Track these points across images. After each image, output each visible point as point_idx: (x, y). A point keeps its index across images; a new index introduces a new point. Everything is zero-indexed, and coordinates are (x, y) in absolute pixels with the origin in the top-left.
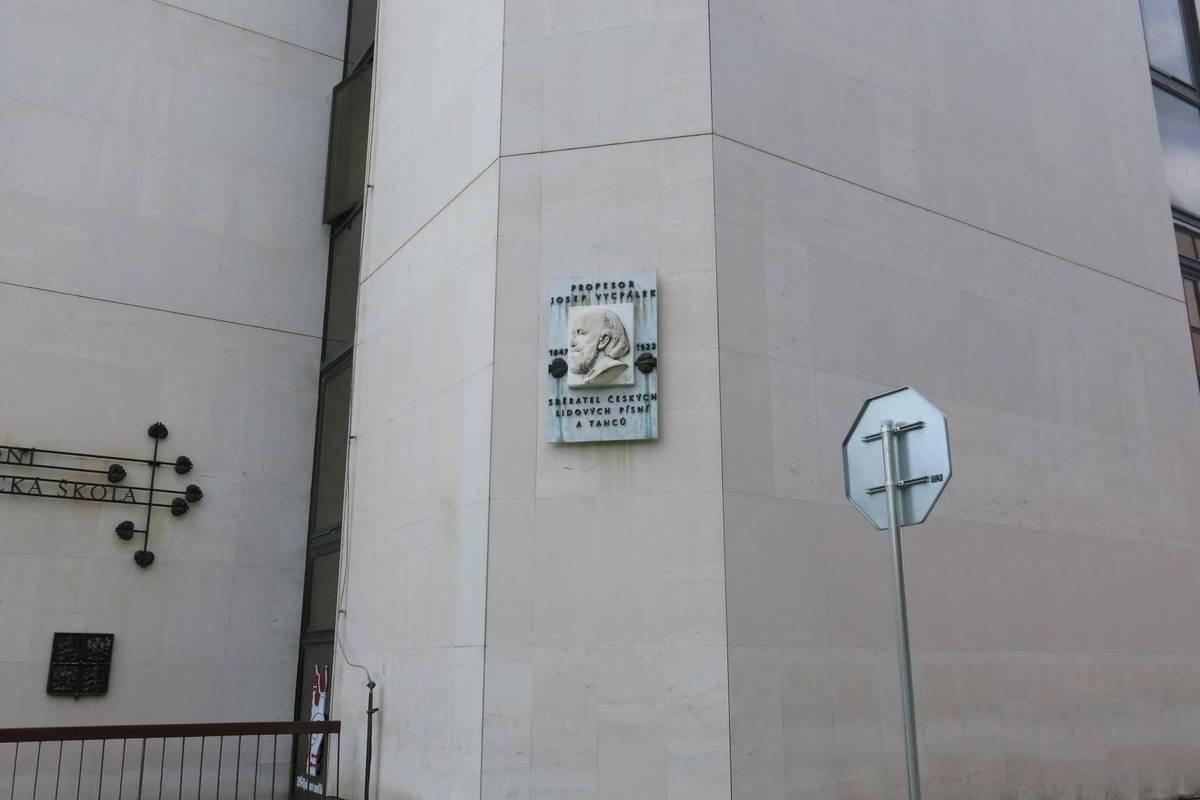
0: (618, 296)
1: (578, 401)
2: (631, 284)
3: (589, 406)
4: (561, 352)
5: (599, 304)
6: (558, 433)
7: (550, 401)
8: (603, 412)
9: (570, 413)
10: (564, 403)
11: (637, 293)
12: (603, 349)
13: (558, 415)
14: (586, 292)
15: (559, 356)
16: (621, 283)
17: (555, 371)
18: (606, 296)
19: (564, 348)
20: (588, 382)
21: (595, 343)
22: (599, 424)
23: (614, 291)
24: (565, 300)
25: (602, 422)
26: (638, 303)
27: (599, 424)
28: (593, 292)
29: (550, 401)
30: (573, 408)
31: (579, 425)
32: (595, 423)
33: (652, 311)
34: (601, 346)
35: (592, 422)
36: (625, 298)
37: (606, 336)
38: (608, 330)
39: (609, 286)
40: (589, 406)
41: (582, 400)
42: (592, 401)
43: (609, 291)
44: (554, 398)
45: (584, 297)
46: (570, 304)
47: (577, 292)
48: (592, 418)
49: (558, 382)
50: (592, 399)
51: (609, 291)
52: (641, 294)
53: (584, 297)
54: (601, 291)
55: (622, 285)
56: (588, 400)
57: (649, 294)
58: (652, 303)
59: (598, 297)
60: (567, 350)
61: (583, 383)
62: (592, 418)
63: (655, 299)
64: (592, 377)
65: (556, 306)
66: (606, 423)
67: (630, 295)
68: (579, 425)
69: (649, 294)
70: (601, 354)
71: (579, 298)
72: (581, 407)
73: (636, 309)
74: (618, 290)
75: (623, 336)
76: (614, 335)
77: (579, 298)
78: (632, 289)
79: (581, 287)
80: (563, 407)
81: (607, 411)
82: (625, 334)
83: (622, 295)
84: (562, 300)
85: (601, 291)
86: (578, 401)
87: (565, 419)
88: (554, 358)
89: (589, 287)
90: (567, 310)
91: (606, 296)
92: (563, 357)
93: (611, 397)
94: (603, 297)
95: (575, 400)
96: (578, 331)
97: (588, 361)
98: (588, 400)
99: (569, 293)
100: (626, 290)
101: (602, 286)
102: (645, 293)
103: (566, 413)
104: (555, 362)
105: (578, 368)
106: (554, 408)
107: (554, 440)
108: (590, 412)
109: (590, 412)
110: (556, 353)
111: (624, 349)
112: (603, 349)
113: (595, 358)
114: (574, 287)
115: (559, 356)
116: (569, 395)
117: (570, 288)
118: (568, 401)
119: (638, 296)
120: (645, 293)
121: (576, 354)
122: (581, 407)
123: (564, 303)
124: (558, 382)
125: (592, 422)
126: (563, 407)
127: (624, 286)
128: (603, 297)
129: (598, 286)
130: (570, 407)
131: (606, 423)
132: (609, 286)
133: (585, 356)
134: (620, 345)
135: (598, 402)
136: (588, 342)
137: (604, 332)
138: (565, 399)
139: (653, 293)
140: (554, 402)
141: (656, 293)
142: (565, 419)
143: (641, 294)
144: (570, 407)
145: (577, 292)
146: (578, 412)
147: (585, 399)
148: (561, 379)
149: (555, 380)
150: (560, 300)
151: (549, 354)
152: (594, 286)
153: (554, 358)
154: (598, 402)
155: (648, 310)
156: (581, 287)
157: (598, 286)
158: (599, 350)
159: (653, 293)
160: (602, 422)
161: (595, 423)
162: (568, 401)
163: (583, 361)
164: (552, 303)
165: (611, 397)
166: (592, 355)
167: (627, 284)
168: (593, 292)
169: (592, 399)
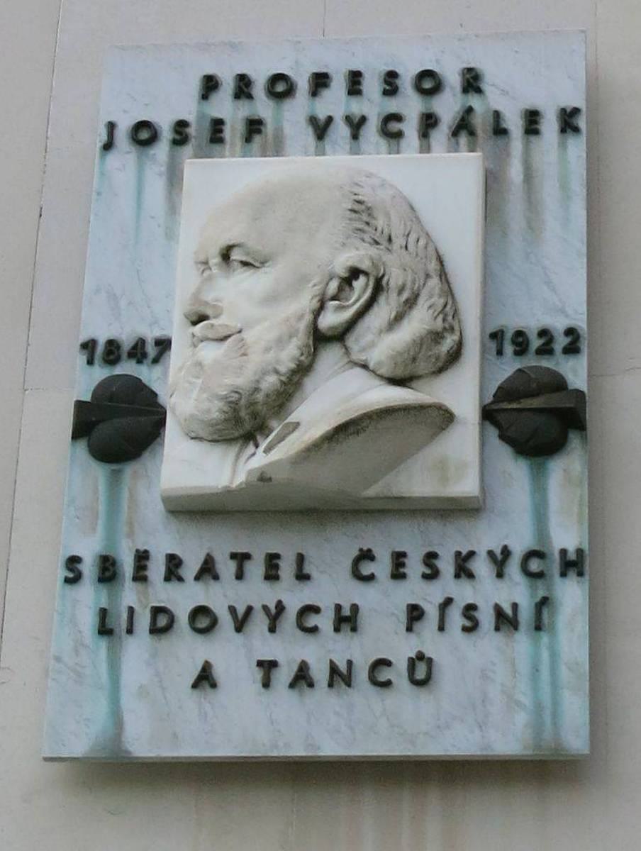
0: (410, 128)
1: (208, 570)
2: (472, 81)
3: (257, 592)
4: (138, 352)
5: (320, 152)
6: (99, 710)
7: (73, 562)
8: (325, 621)
9: (162, 623)
10: (140, 576)
11: (497, 115)
12: (340, 336)
13: (105, 630)
14: (263, 107)
15: (127, 368)
16: (426, 74)
17: (104, 430)
18: (356, 125)
19: (151, 334)
20: (263, 478)
21: (306, 302)
22: (302, 677)
23: (393, 105)
24: (167, 134)
25: (320, 673)
26: (505, 154)
27: (302, 677)
28: (299, 107)
29: (73, 562)
30: (182, 598)
31: (205, 678)
32: (284, 675)
33: (564, 186)
34: (331, 319)
35: (268, 667)
36: (440, 135)
37: (355, 273)
38: (373, 251)
39: (372, 86)
40: (257, 592)
41: (226, 568)
42: (272, 575)
43: (372, 105)
44: (89, 551)
45: (254, 127)
46: (188, 149)
47: (224, 106)
48: (269, 647)
49: (115, 482)
50: (272, 562)
51: (372, 105)
52: (515, 124)
53: (254, 127)
54: (334, 102)
55: (429, 83)
56: (256, 569)
57: (550, 125)
58: (563, 160)
59: (321, 129)
60: (164, 345)
61: (240, 478)
62: (269, 647)
63: (577, 148)
64: (278, 454)
65: (125, 151)
66: (340, 677)
67: (464, 126)
68: (205, 678)
69: (550, 125)
70: (330, 356)
71: (233, 131)
72: (219, 597)
73: (492, 183)
74: (411, 105)
75: (434, 282)
76: (395, 277)
77: (233, 131)
78: (474, 101)
79: (243, 87)
80: (129, 595)
81: (347, 620)
82: (443, 275)
83: (429, 122)
84: (154, 138)
85: (334, 102)
86: (208, 570)
87: (138, 648)
88: (100, 373)
89: (280, 87)
90: (174, 177)
91: (356, 125)
92: (146, 374)
93: (367, 555)
94: (341, 131)
95: (191, 567)
96: (226, 255)
97: (271, 382)
98: (256, 569)
99: (187, 107)
100: (448, 106)
101: (339, 85)
102: (532, 120)
103: (143, 621)
104: (103, 390)
105: (216, 410)
106: (89, 596)
107: (79, 746)
108: (259, 623)
109: (259, 623)
110: (113, 352)
111: (437, 337)
112: (340, 336)
113: (302, 370)
114: (210, 85)
115: (127, 368)
116: (162, 541)
117: (195, 86)
118: (157, 569)
119: (500, 131)
120: (532, 120)
121: (210, 353)
122: (219, 597)
123: (162, 150)
124: (115, 482)
125: (268, 667)
126: (129, 595)
127: (437, 88)
128: (341, 131)
129: (320, 81)
130: (162, 593)
131: (340, 677)
132: (372, 86)
133: (256, 360)
134: (419, 322)
135: (302, 577)
136: (272, 299)
137: (342, 263)
138: (142, 558)
139: (568, 121)
140: (89, 568)
141: (582, 122)
142: (138, 648)
143: (515, 124)
144: (162, 593)
145: (224, 106)
146: (203, 620)
147: (241, 559)
148: (129, 469)
149: (99, 472)
150: (144, 134)
151: (82, 359)
152: (303, 85)
153: (100, 373)
154: (302, 577)
155: (549, 191)
156: (243, 87)
157: (320, 81)
158: (319, 339)
159: (568, 121)
160: (320, 673)
161: (284, 675)
162: (157, 569)
163: (243, 380)
164: (108, 146)
165: (367, 555)
166: (288, 356)
167: (453, 79)
168: (298, 108)
169: (272, 562)
